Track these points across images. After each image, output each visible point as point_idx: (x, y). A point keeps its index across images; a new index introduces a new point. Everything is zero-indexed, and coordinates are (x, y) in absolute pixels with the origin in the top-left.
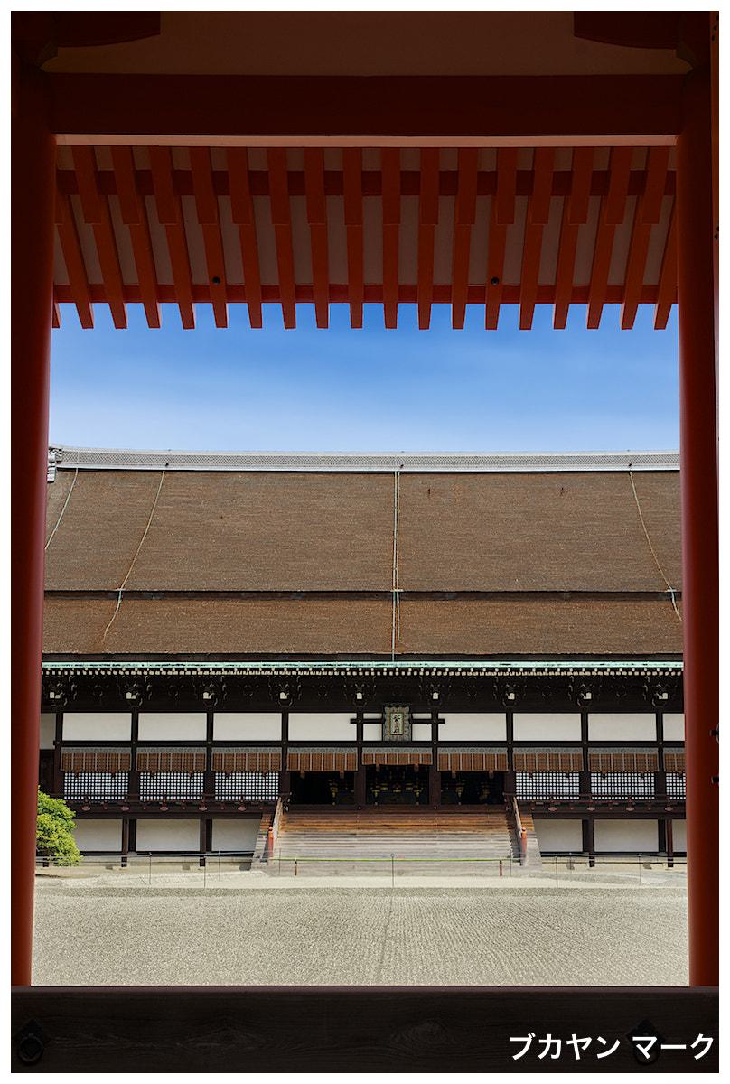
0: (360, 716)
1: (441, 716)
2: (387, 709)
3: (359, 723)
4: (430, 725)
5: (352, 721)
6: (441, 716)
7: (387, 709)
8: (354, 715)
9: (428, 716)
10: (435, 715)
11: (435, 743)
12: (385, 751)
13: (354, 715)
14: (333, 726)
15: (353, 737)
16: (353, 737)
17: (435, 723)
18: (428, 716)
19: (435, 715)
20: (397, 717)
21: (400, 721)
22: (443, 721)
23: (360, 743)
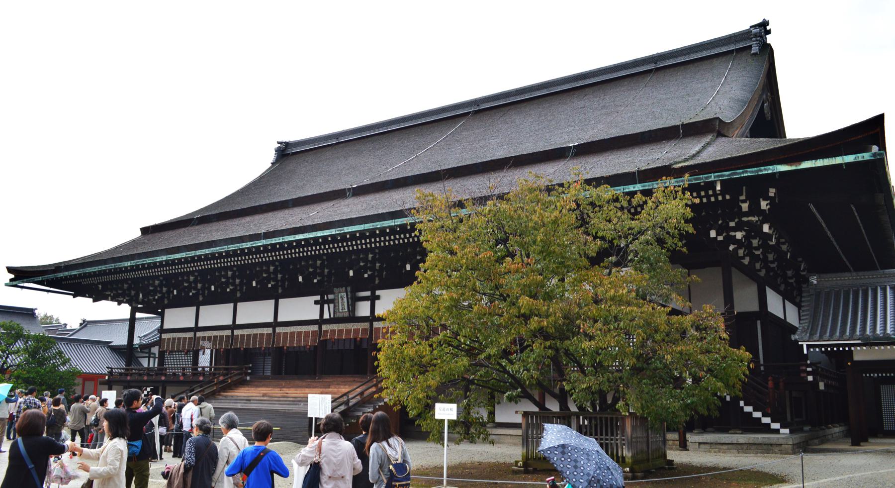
0: (322, 297)
1: (378, 293)
2: (336, 290)
3: (321, 303)
4: (369, 302)
5: (316, 302)
6: (378, 293)
7: (336, 290)
8: (318, 298)
9: (368, 293)
10: (373, 293)
11: (373, 318)
12: (335, 327)
13: (318, 298)
14: (301, 309)
15: (317, 317)
16: (317, 317)
17: (373, 299)
18: (368, 293)
19: (373, 293)
20: (342, 298)
21: (345, 300)
22: (378, 298)
23: (321, 322)
